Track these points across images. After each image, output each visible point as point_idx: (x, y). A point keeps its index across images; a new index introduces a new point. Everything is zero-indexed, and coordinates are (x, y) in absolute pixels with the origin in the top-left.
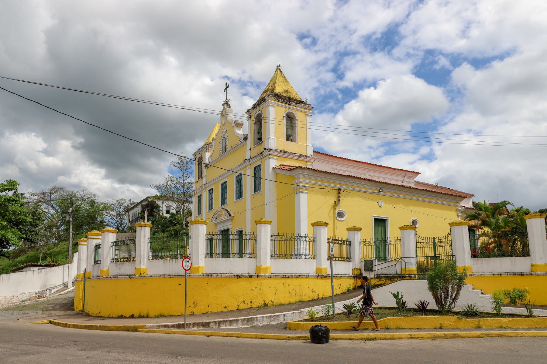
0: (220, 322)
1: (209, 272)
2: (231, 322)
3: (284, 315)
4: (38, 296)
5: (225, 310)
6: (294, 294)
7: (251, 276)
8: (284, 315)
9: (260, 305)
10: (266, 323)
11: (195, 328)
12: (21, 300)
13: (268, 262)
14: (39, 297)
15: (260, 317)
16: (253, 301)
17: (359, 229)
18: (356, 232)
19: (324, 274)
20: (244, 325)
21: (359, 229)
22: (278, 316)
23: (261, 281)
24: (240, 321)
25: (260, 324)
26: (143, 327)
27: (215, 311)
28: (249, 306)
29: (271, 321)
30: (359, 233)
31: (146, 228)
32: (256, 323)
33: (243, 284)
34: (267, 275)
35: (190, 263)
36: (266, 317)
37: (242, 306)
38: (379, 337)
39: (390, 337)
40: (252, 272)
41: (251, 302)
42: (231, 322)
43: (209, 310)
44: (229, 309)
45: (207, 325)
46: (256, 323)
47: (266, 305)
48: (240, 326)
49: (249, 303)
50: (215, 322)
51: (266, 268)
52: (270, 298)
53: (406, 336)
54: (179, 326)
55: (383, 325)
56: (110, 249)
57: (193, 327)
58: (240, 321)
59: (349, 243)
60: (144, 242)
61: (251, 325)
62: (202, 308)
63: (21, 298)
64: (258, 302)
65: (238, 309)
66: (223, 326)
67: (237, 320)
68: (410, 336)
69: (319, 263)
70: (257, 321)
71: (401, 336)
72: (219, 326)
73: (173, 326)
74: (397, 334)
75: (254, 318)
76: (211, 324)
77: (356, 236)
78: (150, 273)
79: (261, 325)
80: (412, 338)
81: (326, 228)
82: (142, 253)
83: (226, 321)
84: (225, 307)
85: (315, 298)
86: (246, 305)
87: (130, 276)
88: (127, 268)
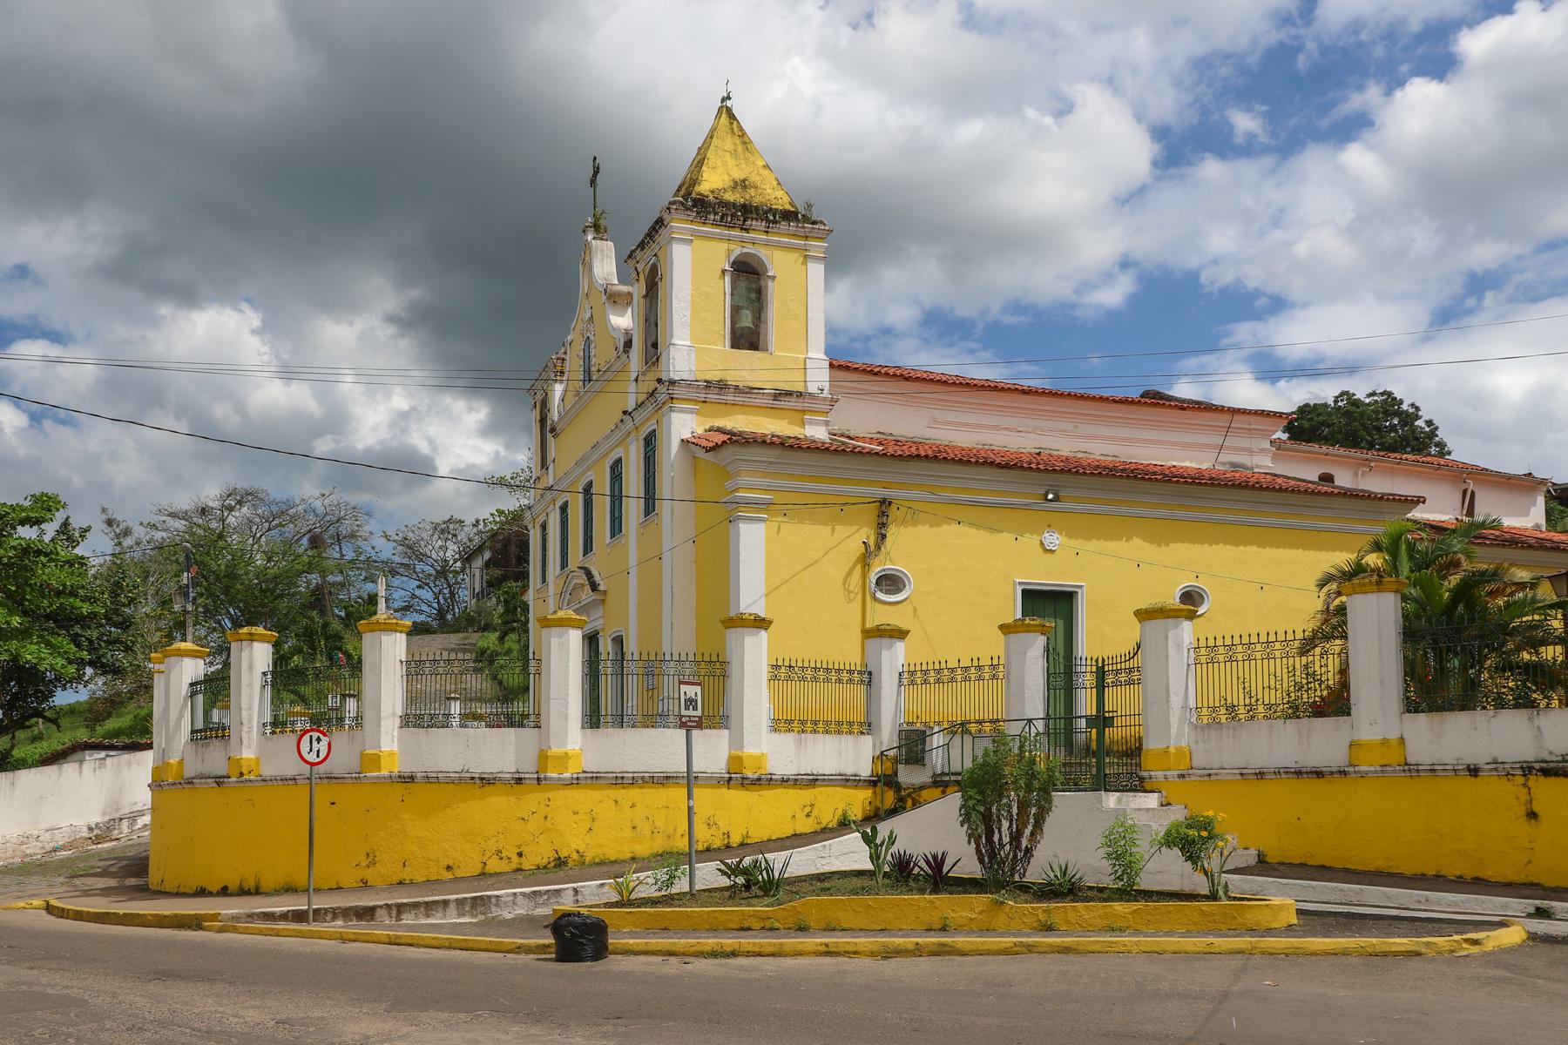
0: (401, 908)
1: (407, 769)
2: (429, 907)
3: (576, 891)
4: (97, 836)
5: (449, 875)
6: (648, 832)
7: (519, 781)
8: (576, 891)
9: (545, 861)
10: (523, 912)
11: (339, 923)
12: (49, 847)
13: (570, 738)
14: (98, 840)
15: (508, 895)
16: (526, 850)
17: (901, 634)
18: (885, 641)
19: (749, 775)
20: (461, 915)
21: (901, 634)
22: (558, 891)
23: (550, 795)
24: (453, 906)
25: (508, 915)
26: (215, 917)
27: (420, 879)
28: (514, 866)
29: (537, 905)
30: (900, 647)
31: (256, 644)
32: (495, 912)
33: (499, 803)
34: (567, 775)
35: (325, 741)
36: (524, 894)
37: (494, 865)
38: (745, 948)
39: (772, 950)
40: (528, 767)
41: (520, 855)
42: (429, 907)
43: (406, 875)
44: (459, 874)
45: (367, 913)
46: (495, 912)
47: (560, 863)
48: (452, 918)
49: (515, 858)
50: (388, 906)
51: (565, 758)
52: (575, 842)
53: (813, 948)
54: (299, 916)
55: (791, 920)
56: (184, 706)
57: (334, 918)
58: (453, 906)
59: (868, 678)
60: (251, 685)
61: (481, 917)
62: (389, 869)
63: (48, 841)
64: (539, 854)
65: (483, 874)
66: (408, 919)
67: (446, 903)
68: (823, 948)
69: (737, 741)
70: (497, 905)
71: (800, 948)
72: (399, 918)
73: (284, 917)
74: (791, 942)
75: (489, 897)
76: (379, 912)
77: (885, 654)
78: (267, 771)
79: (508, 916)
80: (828, 954)
81: (763, 634)
82: (244, 714)
83: (416, 905)
84: (449, 868)
85: (717, 843)
86: (505, 861)
87: (220, 780)
88: (214, 759)
